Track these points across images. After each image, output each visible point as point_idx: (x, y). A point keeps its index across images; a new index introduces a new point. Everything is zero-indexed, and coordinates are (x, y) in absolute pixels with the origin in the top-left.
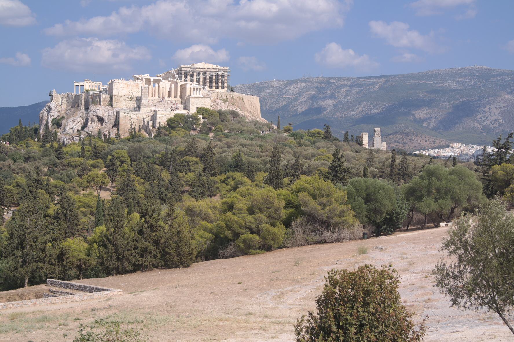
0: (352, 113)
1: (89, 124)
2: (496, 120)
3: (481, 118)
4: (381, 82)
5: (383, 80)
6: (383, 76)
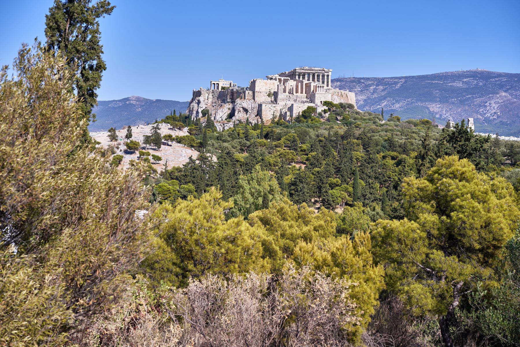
0: (378, 107)
1: (236, 114)
2: (495, 113)
3: (483, 111)
4: (401, 82)
5: (403, 80)
6: (403, 77)
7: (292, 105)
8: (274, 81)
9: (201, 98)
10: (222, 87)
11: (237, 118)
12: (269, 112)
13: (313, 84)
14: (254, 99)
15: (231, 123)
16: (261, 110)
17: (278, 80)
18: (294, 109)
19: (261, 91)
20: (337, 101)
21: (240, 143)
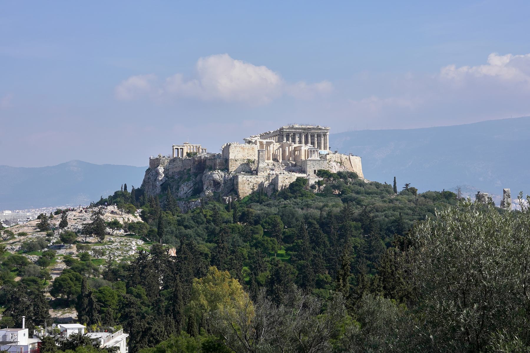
1: (205, 188)
10: (187, 153)
12: (247, 186)
17: (258, 144)
18: (280, 182)
19: (236, 158)
20: (335, 169)
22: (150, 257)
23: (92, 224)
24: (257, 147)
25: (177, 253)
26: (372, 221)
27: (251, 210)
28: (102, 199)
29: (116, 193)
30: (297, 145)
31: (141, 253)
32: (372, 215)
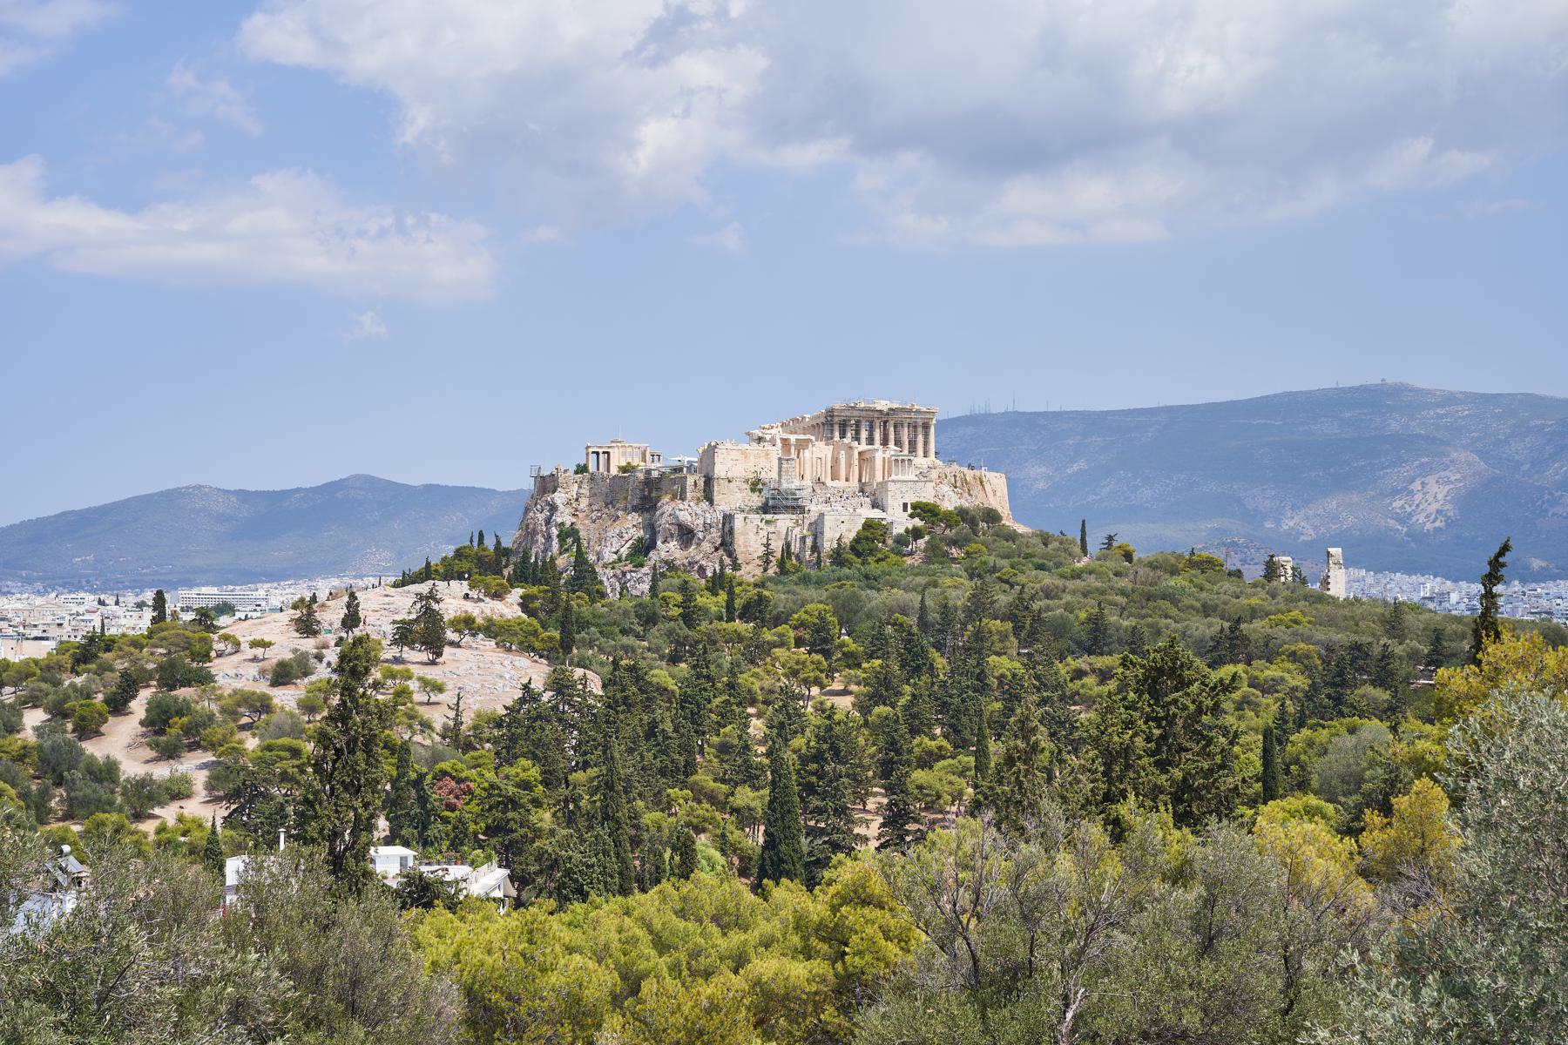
7: (822, 515)
8: (768, 447)
9: (559, 498)
11: (663, 554)
13: (879, 456)
14: (711, 502)
15: (646, 570)
16: (731, 531)
18: (826, 529)
19: (730, 475)
20: (950, 502)
21: (670, 633)
22: (546, 697)
23: (416, 621)
24: (776, 451)
25: (604, 686)
26: (1037, 618)
27: (766, 593)
28: (428, 564)
29: (457, 551)
30: (864, 447)
31: (526, 687)
32: (1036, 606)
